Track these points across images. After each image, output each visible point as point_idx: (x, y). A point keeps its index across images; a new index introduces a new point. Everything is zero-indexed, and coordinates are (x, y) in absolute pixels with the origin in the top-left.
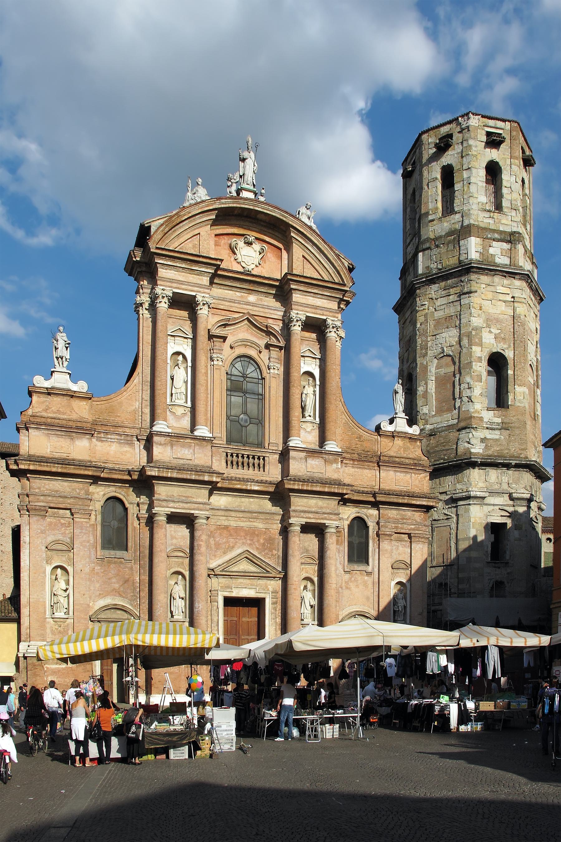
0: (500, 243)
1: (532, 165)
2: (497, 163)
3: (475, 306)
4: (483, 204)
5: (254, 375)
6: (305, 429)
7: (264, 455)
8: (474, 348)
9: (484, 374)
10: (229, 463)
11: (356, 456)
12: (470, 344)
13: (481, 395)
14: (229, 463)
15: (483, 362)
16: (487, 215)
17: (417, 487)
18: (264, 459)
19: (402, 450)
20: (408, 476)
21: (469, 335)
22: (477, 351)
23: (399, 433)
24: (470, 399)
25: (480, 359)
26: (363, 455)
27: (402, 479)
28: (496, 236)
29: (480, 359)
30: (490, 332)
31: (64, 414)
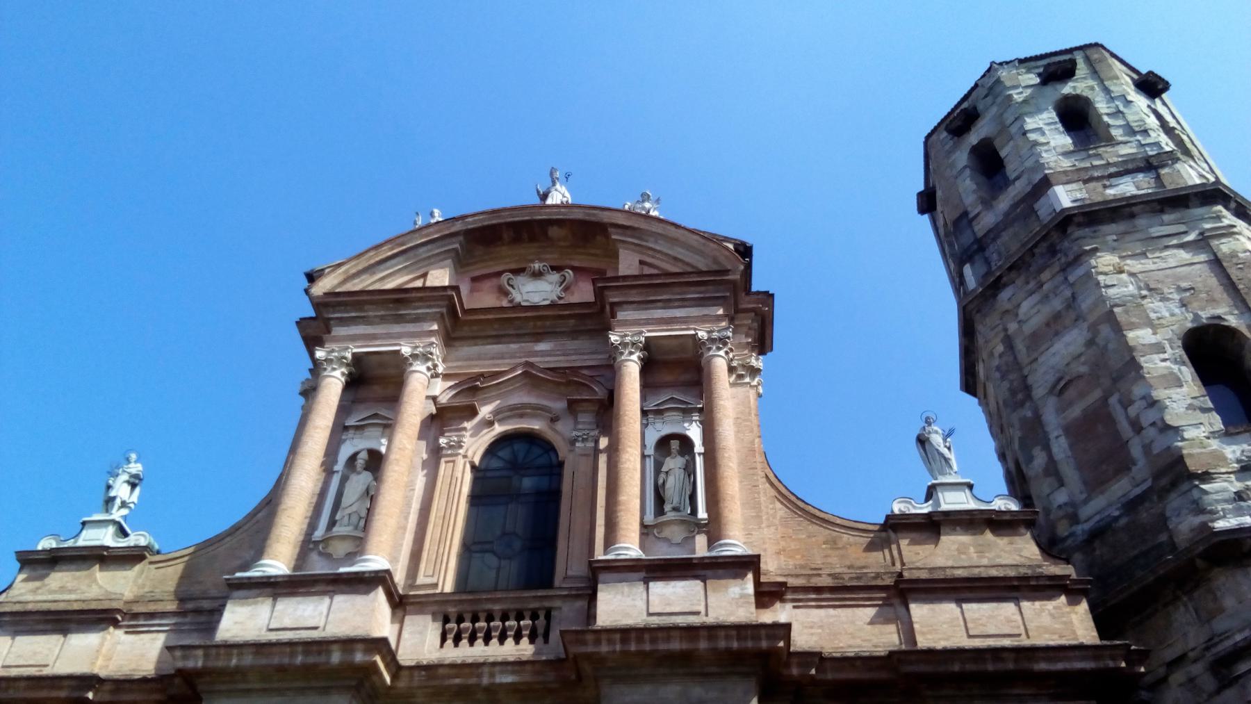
0: (1127, 179)
1: (1166, 86)
2: (1077, 98)
3: (1106, 269)
4: (1064, 146)
5: (542, 461)
6: (666, 540)
7: (547, 604)
8: (1131, 335)
9: (1187, 373)
10: (451, 636)
11: (825, 581)
12: (1118, 329)
13: (1190, 407)
14: (451, 636)
15: (1169, 350)
16: (1083, 154)
17: (1047, 630)
18: (548, 617)
19: (972, 549)
20: (1008, 608)
21: (1110, 317)
22: (1139, 336)
23: (947, 514)
24: (1166, 428)
25: (1158, 348)
26: (846, 577)
27: (990, 617)
28: (1112, 170)
29: (1158, 348)
30: (1164, 299)
31: (71, 592)
